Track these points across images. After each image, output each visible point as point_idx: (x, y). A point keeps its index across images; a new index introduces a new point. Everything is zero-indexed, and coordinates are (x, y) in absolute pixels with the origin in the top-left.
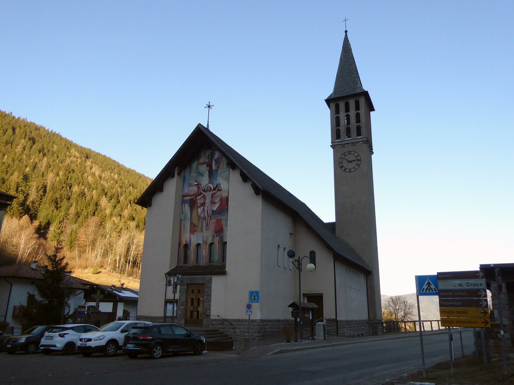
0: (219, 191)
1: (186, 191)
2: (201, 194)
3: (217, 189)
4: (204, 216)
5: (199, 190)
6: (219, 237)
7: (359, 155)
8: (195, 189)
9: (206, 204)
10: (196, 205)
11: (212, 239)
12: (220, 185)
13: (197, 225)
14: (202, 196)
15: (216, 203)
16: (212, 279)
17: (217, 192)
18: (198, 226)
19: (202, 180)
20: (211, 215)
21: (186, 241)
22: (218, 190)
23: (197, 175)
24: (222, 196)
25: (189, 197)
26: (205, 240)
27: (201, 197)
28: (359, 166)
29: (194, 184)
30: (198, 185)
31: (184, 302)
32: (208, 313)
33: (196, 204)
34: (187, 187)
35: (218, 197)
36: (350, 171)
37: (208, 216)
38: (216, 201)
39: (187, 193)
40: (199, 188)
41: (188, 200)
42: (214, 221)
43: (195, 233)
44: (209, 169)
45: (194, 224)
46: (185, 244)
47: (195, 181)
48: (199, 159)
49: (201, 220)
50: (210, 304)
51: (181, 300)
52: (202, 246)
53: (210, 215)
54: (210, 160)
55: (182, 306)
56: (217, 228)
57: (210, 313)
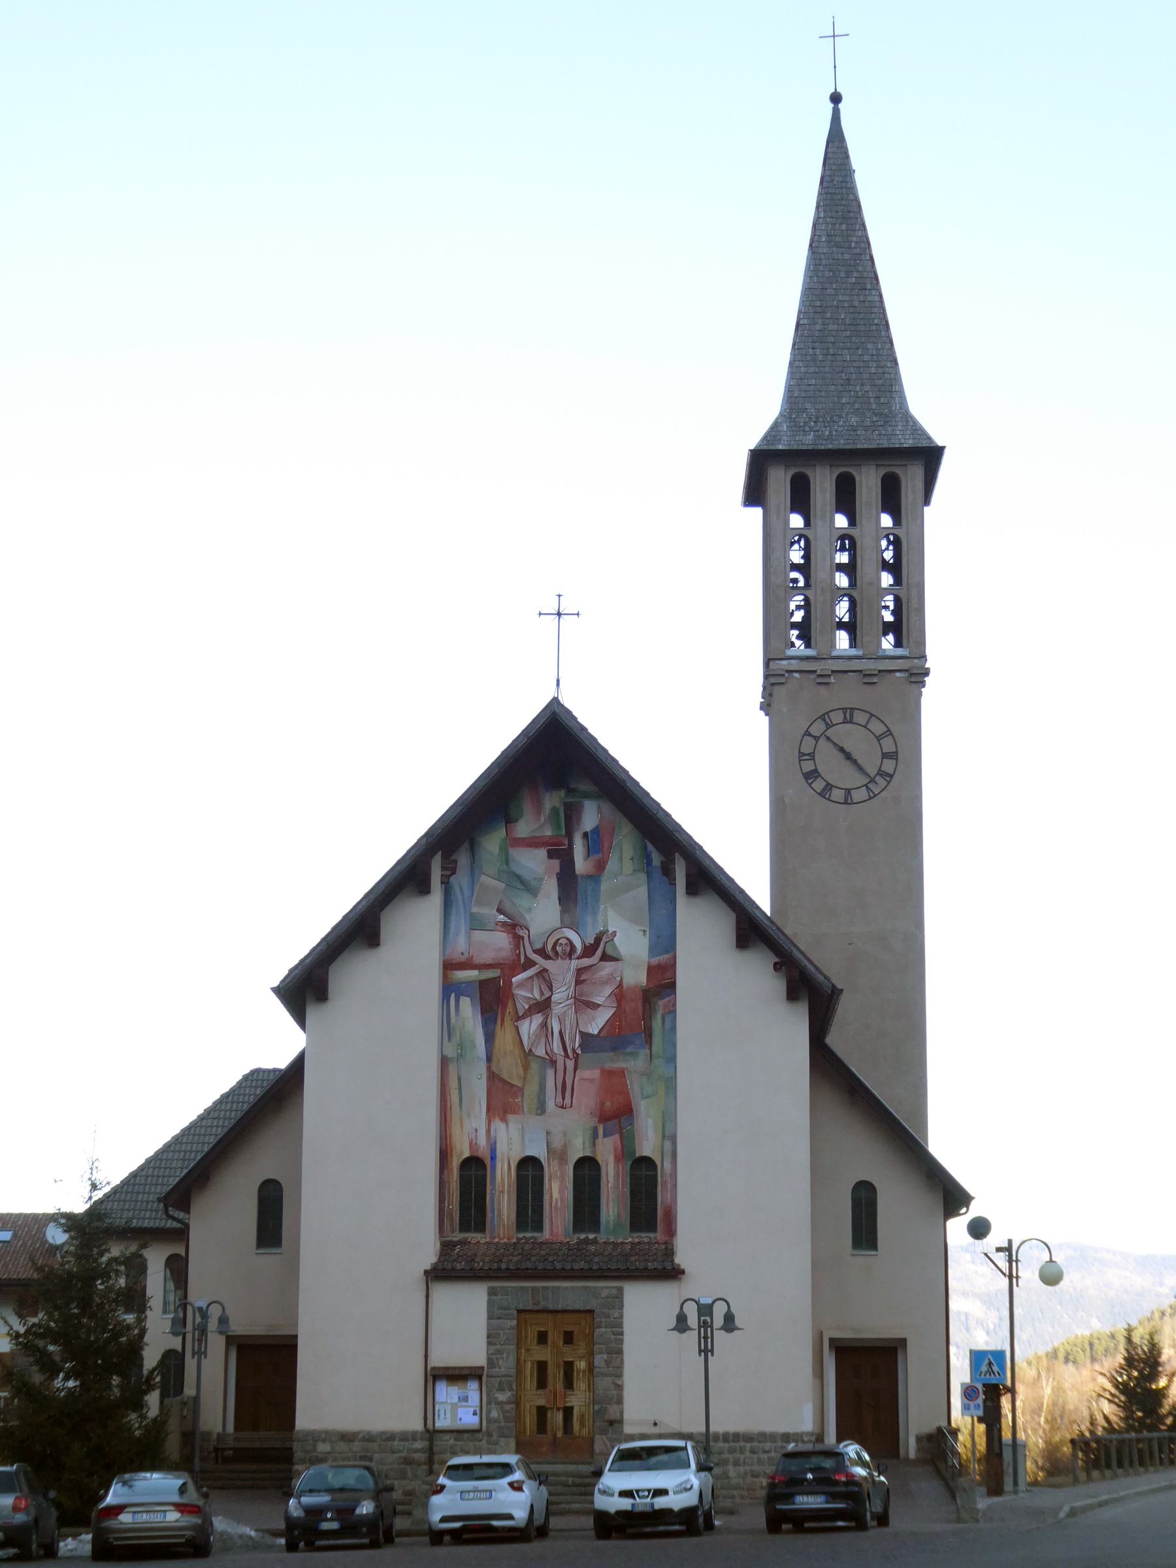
0: (605, 960)
1: (461, 946)
2: (530, 964)
3: (599, 953)
4: (547, 1053)
5: (517, 947)
6: (617, 1137)
7: (889, 733)
9: (552, 1005)
11: (587, 1143)
12: (613, 940)
13: (520, 1085)
14: (536, 974)
15: (596, 1006)
16: (622, 1295)
17: (600, 962)
18: (521, 1090)
19: (529, 910)
20: (579, 1051)
22: (605, 958)
24: (621, 981)
27: (531, 977)
28: (889, 782)
30: (514, 928)
31: (511, 1376)
32: (612, 1412)
33: (510, 1005)
35: (605, 983)
36: (847, 801)
37: (567, 1056)
38: (599, 1000)
39: (462, 953)
40: (518, 939)
41: (469, 983)
42: (595, 1074)
43: (511, 1117)
44: (561, 869)
46: (467, 1154)
47: (500, 911)
48: (510, 821)
49: (535, 1066)
50: (619, 1383)
51: (497, 1369)
53: (574, 1051)
54: (563, 832)
55: (501, 1389)
56: (608, 1104)
57: (622, 1412)
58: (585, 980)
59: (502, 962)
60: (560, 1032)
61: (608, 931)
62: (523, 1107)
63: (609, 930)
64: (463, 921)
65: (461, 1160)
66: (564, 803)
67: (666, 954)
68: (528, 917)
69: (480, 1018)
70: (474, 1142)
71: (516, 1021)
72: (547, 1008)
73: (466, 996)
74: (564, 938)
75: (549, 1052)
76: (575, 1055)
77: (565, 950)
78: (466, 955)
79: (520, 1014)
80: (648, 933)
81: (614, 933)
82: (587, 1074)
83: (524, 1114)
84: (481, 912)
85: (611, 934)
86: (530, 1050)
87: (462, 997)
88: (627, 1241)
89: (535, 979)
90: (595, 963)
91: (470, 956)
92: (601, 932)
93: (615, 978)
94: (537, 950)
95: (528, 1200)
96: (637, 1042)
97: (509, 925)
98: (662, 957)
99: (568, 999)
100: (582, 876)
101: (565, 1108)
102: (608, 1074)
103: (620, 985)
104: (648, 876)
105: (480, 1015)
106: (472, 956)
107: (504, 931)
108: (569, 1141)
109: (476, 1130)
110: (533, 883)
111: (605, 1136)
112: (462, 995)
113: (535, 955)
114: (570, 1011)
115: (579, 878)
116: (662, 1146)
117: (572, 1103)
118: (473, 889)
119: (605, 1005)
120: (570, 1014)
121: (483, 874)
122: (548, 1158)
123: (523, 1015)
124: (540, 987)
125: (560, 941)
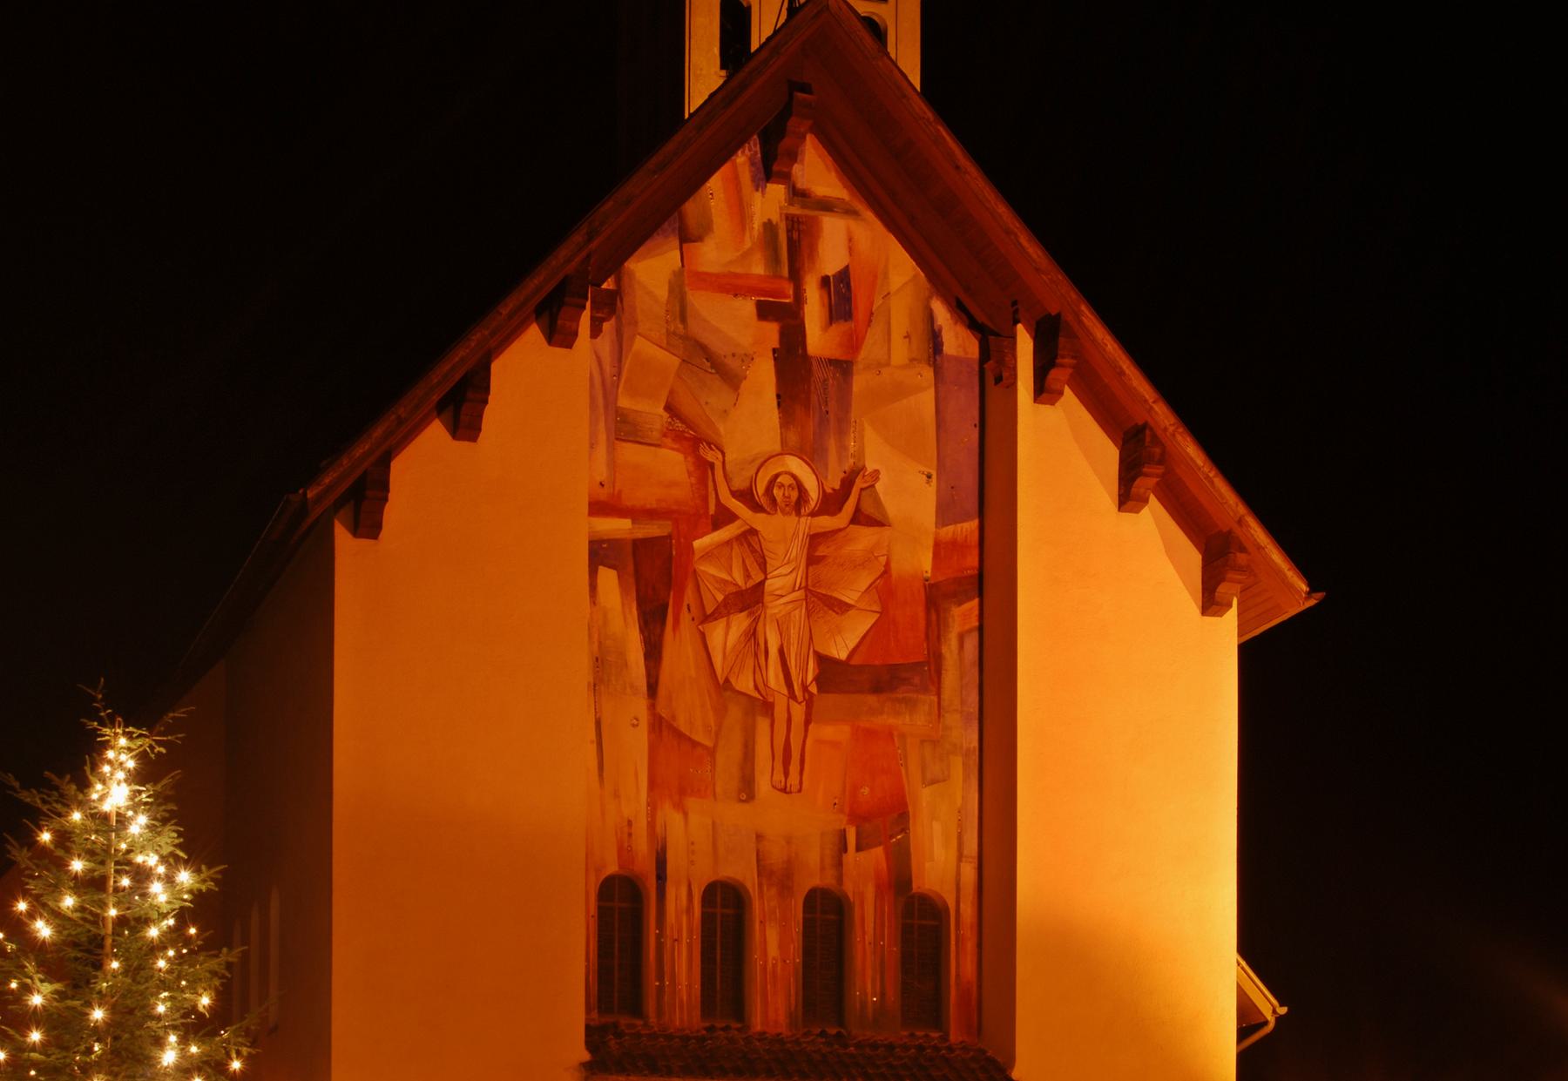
2: (724, 517)
4: (756, 688)
5: (703, 482)
8: (672, 464)
9: (767, 598)
10: (689, 596)
12: (873, 486)
13: (709, 743)
15: (843, 608)
18: (712, 752)
20: (814, 689)
22: (859, 518)
23: (684, 360)
24: (887, 565)
25: (625, 524)
26: (776, 855)
27: (728, 543)
34: (602, 437)
37: (792, 695)
38: (850, 597)
40: (704, 468)
43: (692, 803)
44: (781, 342)
45: (680, 735)
46: (612, 868)
52: (756, 904)
53: (805, 688)
54: (785, 271)
56: (866, 791)
58: (824, 557)
59: (675, 507)
60: (781, 652)
61: (864, 468)
62: (714, 785)
63: (867, 466)
66: (787, 218)
69: (635, 613)
70: (626, 844)
71: (702, 622)
72: (758, 603)
73: (611, 567)
74: (786, 473)
76: (807, 697)
77: (789, 497)
79: (709, 612)
80: (934, 477)
83: (715, 800)
85: (870, 474)
87: (601, 568)
89: (735, 546)
90: (842, 527)
91: (616, 492)
93: (876, 558)
94: (737, 491)
96: (916, 680)
98: (959, 525)
99: (794, 591)
100: (820, 360)
101: (791, 792)
102: (867, 736)
104: (936, 373)
106: (620, 492)
109: (630, 823)
110: (733, 364)
113: (734, 500)
114: (797, 612)
115: (814, 363)
118: (620, 360)
119: (862, 605)
120: (797, 617)
121: (639, 334)
122: (760, 885)
123: (713, 613)
124: (744, 561)
125: (779, 480)
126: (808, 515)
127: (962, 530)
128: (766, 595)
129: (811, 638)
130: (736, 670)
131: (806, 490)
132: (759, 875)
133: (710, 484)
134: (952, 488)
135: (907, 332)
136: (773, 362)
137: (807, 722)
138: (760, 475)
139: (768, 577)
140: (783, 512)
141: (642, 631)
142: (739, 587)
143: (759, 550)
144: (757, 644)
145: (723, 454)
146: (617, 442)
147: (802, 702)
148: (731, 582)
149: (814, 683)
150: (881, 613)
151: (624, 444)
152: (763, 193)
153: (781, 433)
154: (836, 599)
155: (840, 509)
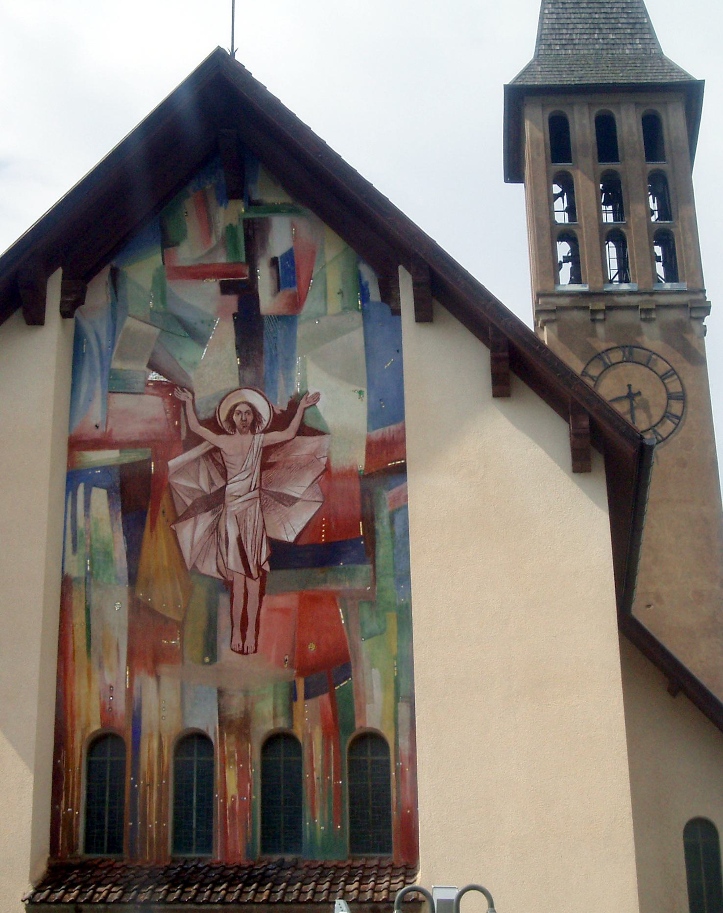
2: (195, 440)
3: (295, 423)
4: (218, 570)
5: (176, 415)
6: (325, 697)
9: (228, 499)
10: (164, 502)
11: (280, 708)
12: (314, 405)
13: (179, 619)
15: (292, 501)
17: (297, 437)
18: (181, 626)
20: (267, 567)
21: (106, 712)
22: (305, 431)
27: (197, 460)
29: (142, 379)
37: (248, 574)
38: (296, 490)
39: (97, 426)
40: (178, 407)
41: (106, 469)
43: (164, 669)
44: (239, 308)
46: (96, 727)
47: (153, 366)
48: (167, 243)
52: (218, 750)
53: (259, 567)
54: (243, 259)
56: (312, 647)
58: (275, 463)
59: (154, 437)
61: (307, 392)
63: (310, 391)
64: (98, 383)
65: (87, 735)
67: (391, 424)
68: (192, 375)
70: (108, 706)
71: (175, 522)
72: (218, 504)
74: (243, 403)
75: (222, 569)
76: (261, 574)
77: (246, 421)
78: (102, 429)
80: (365, 390)
81: (317, 397)
82: (281, 601)
84: (124, 368)
85: (313, 396)
86: (194, 566)
87: (94, 490)
88: (344, 865)
89: (202, 461)
91: (108, 431)
92: (298, 395)
95: (191, 802)
97: (167, 386)
98: (387, 429)
99: (250, 491)
100: (271, 318)
101: (247, 654)
102: (310, 601)
103: (326, 470)
105: (120, 514)
106: (111, 430)
107: (157, 395)
108: (252, 704)
111: (307, 697)
112: (95, 486)
113: (201, 427)
114: (252, 508)
116: (396, 712)
117: (256, 645)
119: (307, 498)
120: (253, 512)
121: (130, 316)
122: (221, 733)
124: (209, 473)
125: (237, 408)
126: (261, 433)
127: (389, 430)
128: (226, 496)
129: (264, 527)
130: (202, 558)
131: (260, 414)
132: (221, 723)
133: (183, 417)
134: (380, 400)
135: (340, 290)
136: (233, 324)
137: (262, 594)
138: (223, 405)
139: (229, 482)
140: (241, 432)
141: (124, 533)
142: (205, 492)
143: (221, 463)
144: (219, 535)
145: (193, 394)
146: (109, 394)
147: (257, 578)
148: (199, 490)
149: (267, 562)
150: (323, 502)
151: (115, 395)
152: (226, 208)
153: (239, 374)
154: (285, 495)
155: (287, 426)
